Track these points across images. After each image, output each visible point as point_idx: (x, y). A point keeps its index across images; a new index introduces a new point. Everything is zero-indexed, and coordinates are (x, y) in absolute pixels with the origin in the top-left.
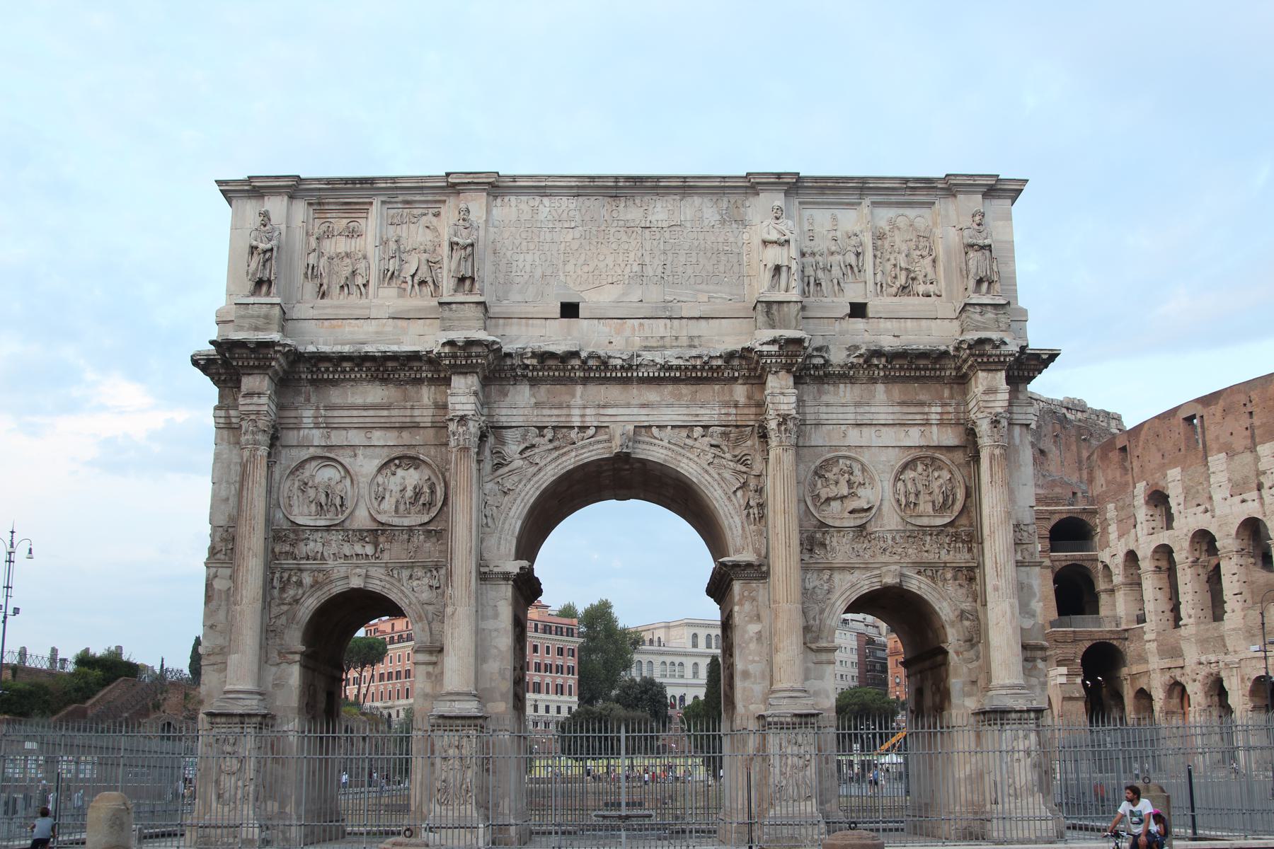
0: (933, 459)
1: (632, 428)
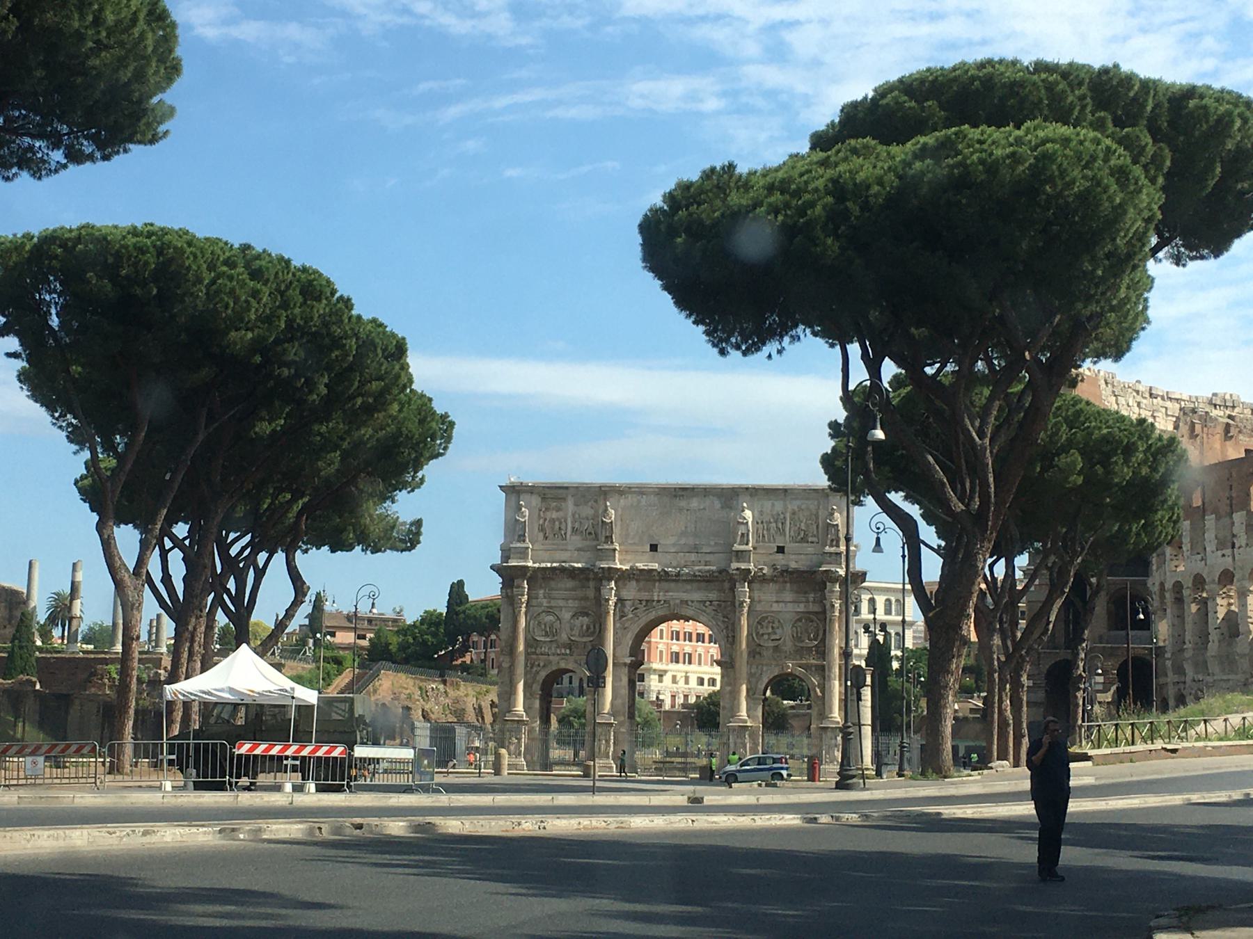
0: (809, 618)
1: (678, 601)
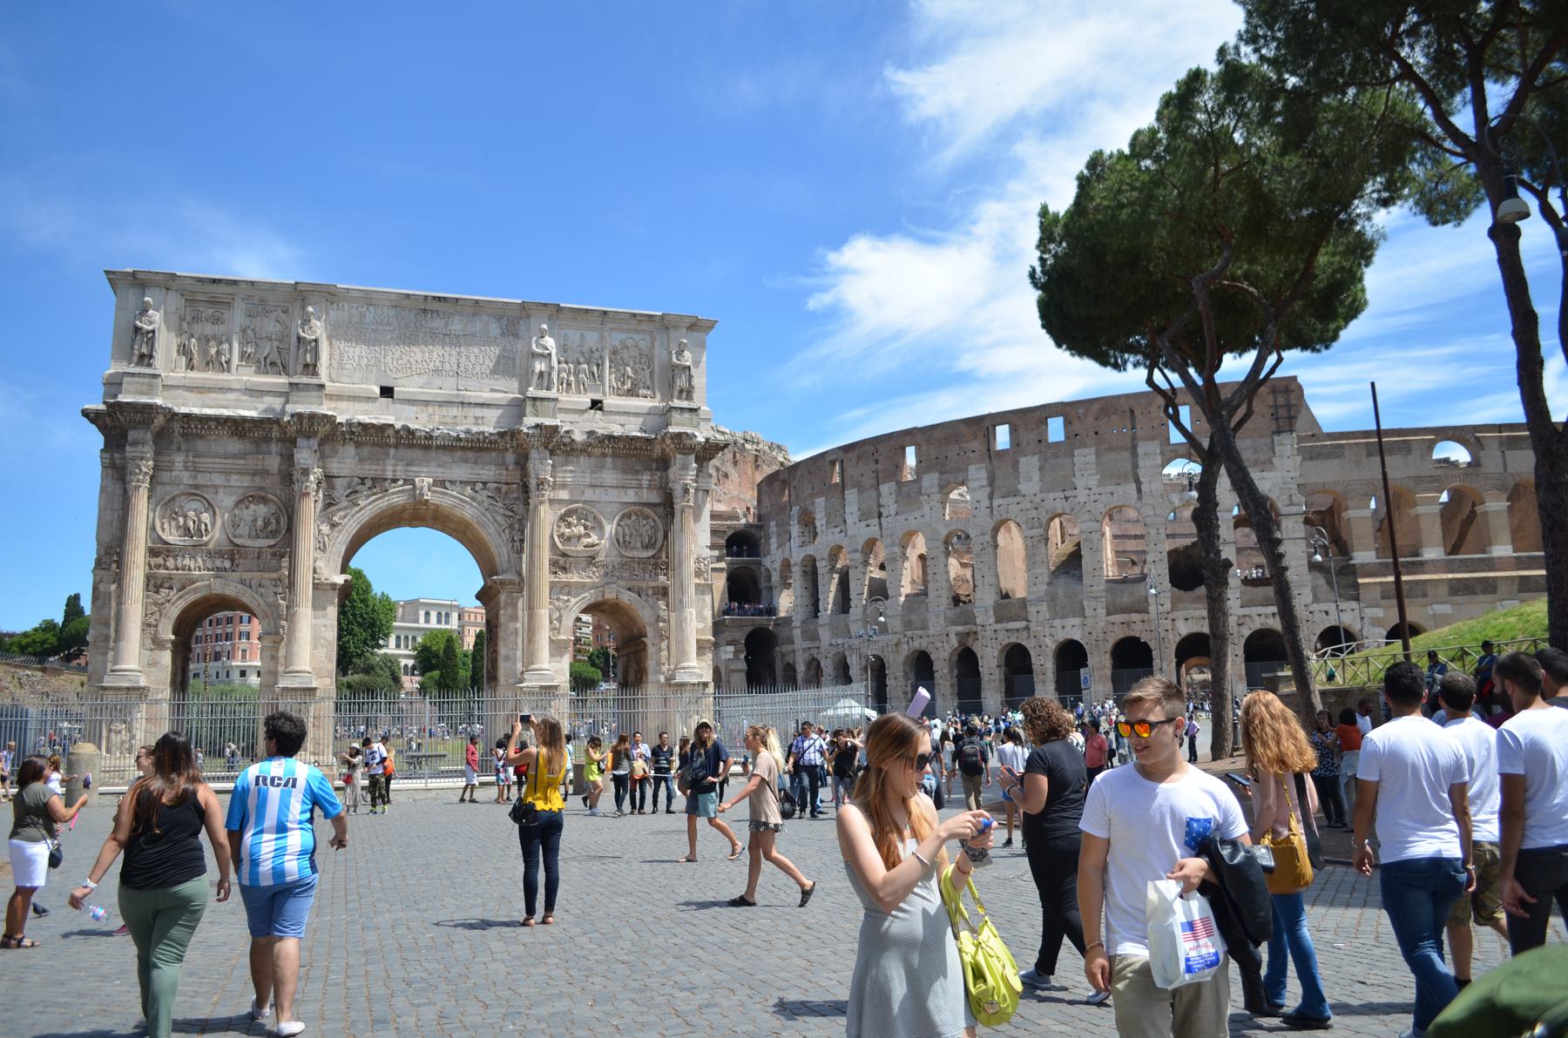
1: (431, 480)
